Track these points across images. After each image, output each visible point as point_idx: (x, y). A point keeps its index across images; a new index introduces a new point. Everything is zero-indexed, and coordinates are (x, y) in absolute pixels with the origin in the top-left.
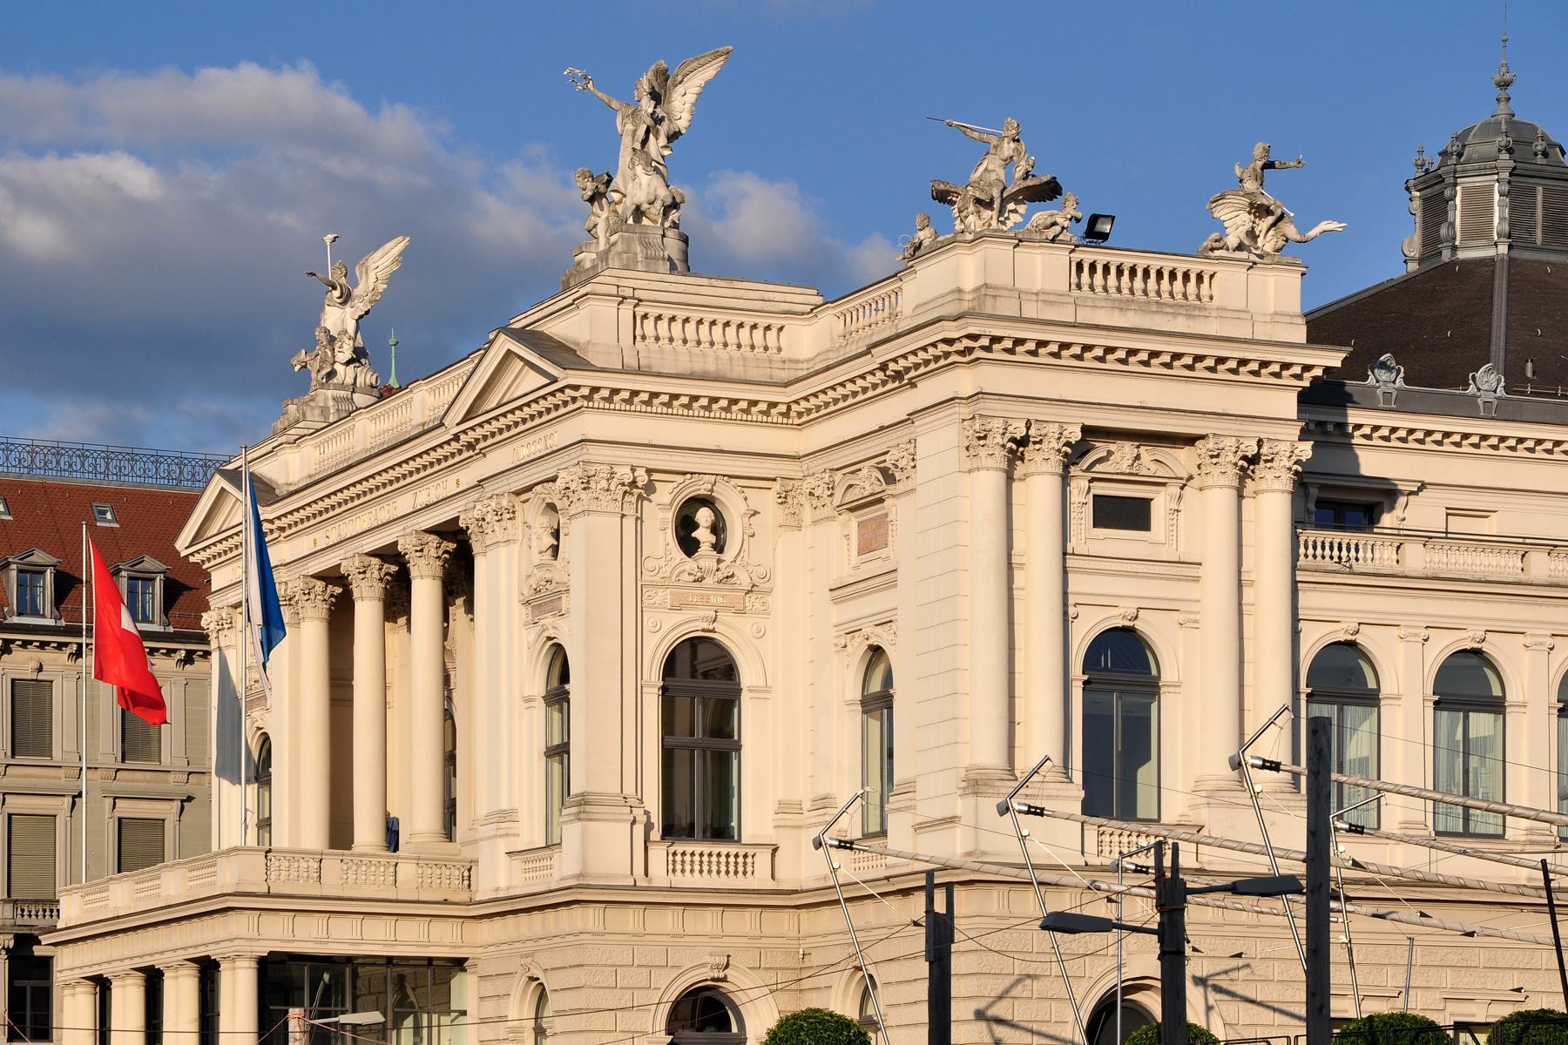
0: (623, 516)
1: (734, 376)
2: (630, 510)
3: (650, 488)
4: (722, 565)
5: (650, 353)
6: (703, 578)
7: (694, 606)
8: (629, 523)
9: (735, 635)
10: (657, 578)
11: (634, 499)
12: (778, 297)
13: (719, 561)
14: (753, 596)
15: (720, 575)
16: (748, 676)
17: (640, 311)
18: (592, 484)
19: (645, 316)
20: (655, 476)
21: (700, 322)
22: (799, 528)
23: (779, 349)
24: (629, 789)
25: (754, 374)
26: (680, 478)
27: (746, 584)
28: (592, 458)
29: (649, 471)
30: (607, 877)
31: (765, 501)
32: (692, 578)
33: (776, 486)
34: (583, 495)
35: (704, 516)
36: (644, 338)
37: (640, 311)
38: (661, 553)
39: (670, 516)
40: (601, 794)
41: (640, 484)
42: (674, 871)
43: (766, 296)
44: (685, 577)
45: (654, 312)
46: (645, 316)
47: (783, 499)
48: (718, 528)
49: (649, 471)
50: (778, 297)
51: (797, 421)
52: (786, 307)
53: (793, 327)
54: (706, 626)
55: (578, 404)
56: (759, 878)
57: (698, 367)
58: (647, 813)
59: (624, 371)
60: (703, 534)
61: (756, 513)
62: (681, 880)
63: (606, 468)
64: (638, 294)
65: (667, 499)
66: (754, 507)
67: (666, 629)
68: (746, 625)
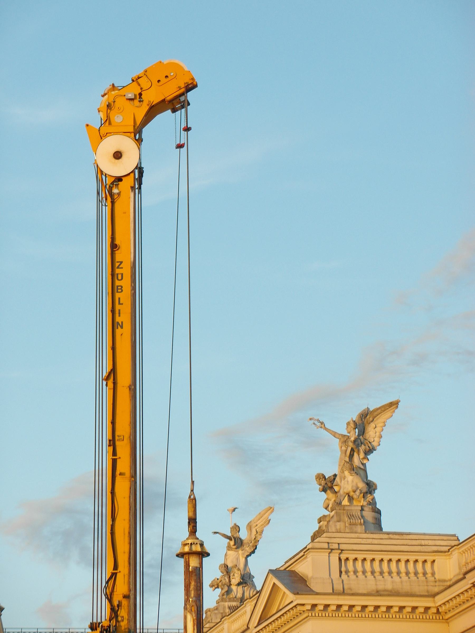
5: (351, 582)
12: (430, 543)
21: (382, 560)
23: (433, 574)
25: (417, 589)
36: (347, 572)
37: (343, 557)
43: (423, 542)
45: (352, 556)
46: (347, 559)
50: (430, 543)
51: (447, 617)
52: (435, 548)
53: (439, 559)
55: (306, 615)
57: (381, 587)
59: (334, 593)
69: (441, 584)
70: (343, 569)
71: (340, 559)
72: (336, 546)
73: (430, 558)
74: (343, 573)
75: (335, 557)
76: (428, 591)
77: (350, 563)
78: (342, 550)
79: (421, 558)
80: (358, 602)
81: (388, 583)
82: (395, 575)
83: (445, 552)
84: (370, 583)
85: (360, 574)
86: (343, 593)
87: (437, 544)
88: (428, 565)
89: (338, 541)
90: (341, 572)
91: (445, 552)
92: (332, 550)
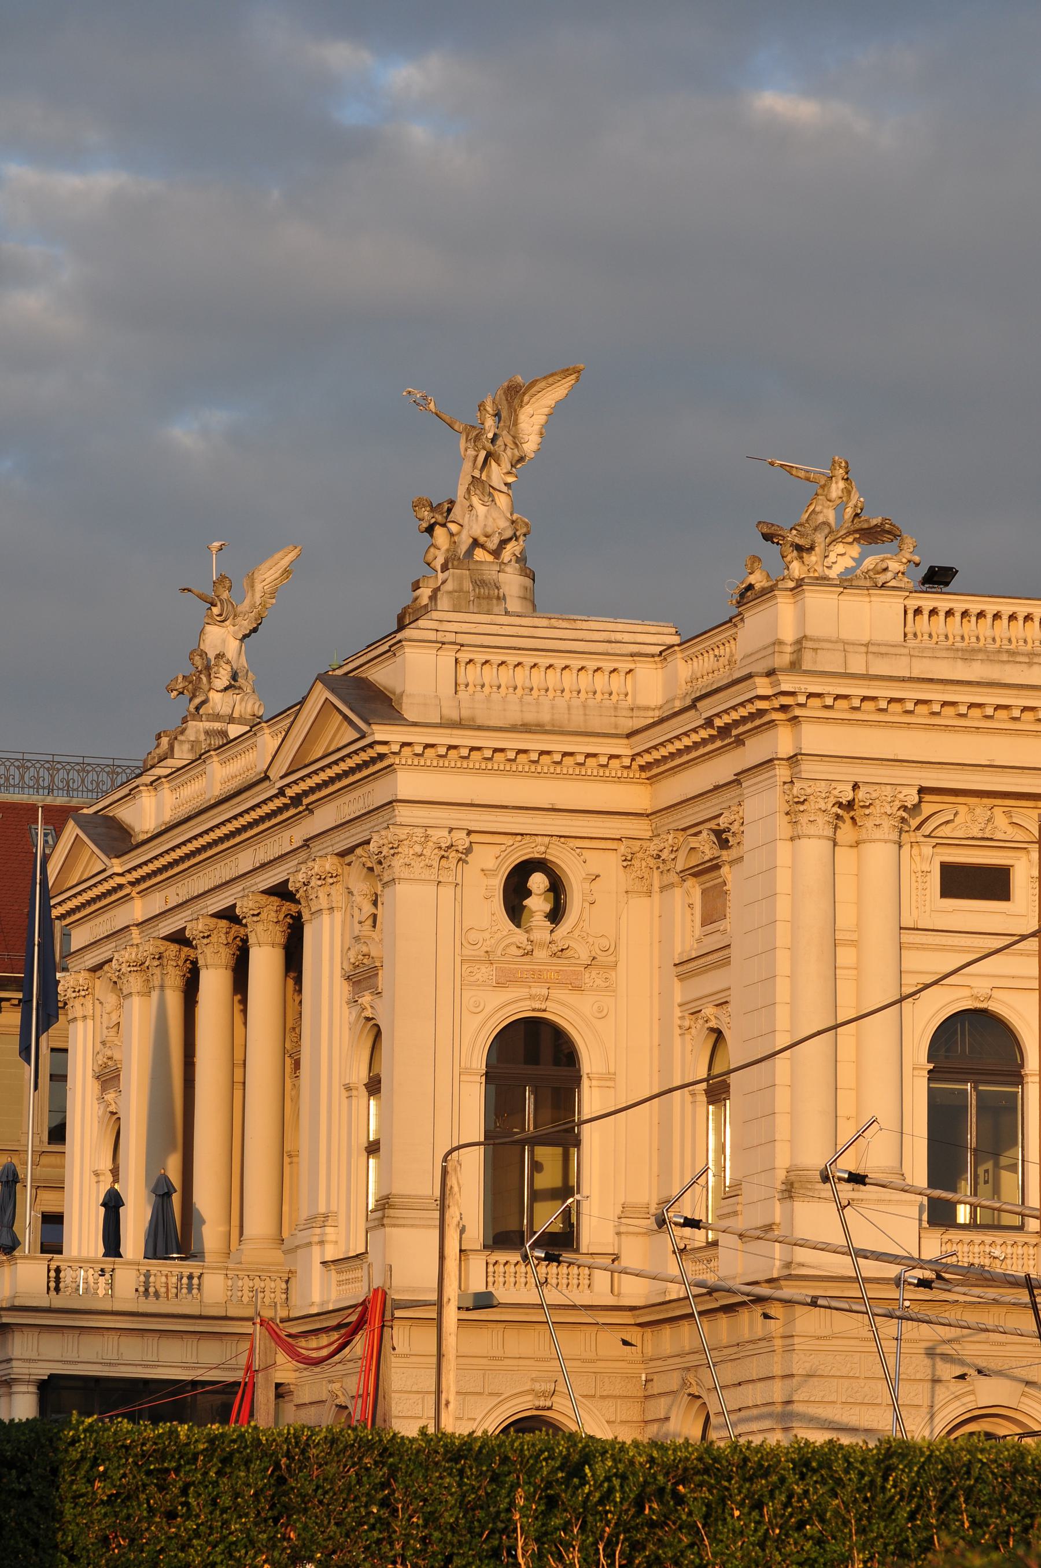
15: (554, 948)
20: (474, 838)
25: (596, 725)
33: (622, 848)
35: (538, 882)
43: (613, 637)
44: (514, 950)
50: (627, 637)
52: (635, 648)
54: (537, 1006)
60: (538, 904)
69: (642, 713)
76: (616, 727)
80: (488, 741)
83: (653, 656)
87: (639, 641)
91: (653, 656)
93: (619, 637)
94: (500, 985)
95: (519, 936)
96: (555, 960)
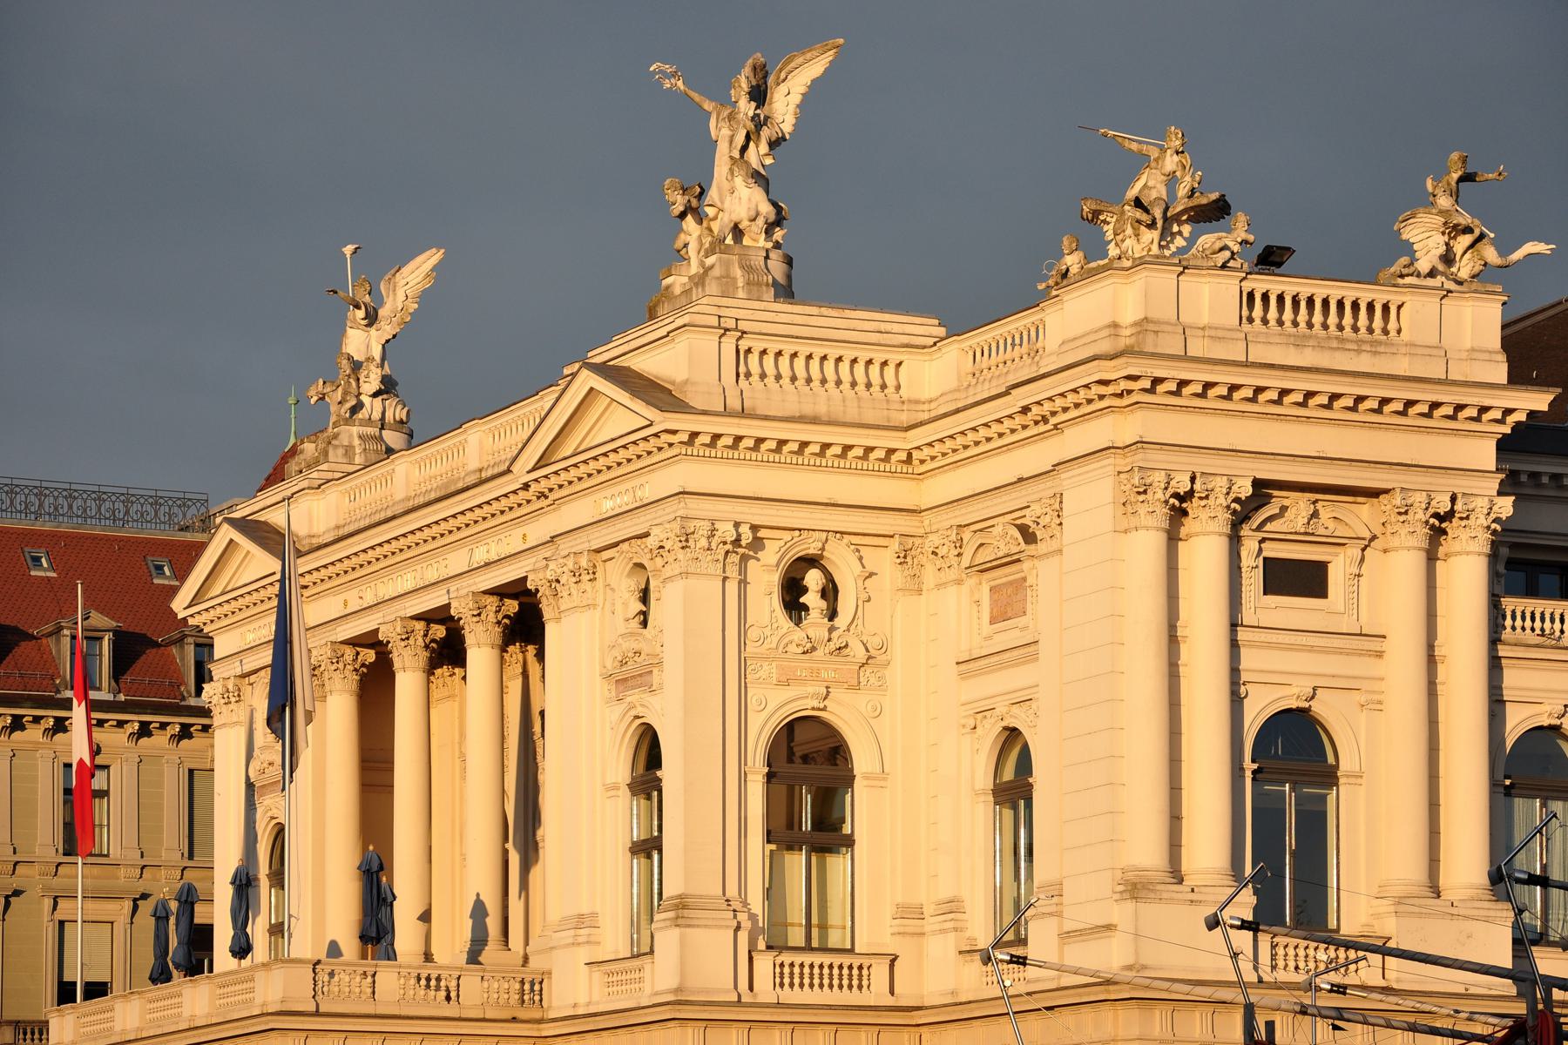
0: (725, 579)
1: (848, 419)
2: (733, 572)
3: (757, 544)
4: (835, 635)
5: (757, 394)
6: (814, 649)
7: (802, 681)
8: (732, 587)
9: (845, 716)
10: (763, 650)
11: (736, 558)
12: (896, 328)
13: (831, 630)
14: (868, 669)
15: (832, 646)
16: (862, 761)
17: (744, 345)
18: (691, 543)
19: (749, 351)
22: (920, 592)
23: (898, 387)
24: (732, 891)
26: (787, 536)
27: (861, 654)
28: (691, 513)
29: (755, 528)
30: (708, 991)
31: (883, 560)
32: (800, 650)
33: (895, 545)
34: (681, 554)
35: (813, 579)
36: (748, 375)
37: (744, 345)
38: (766, 621)
39: (775, 578)
40: (701, 897)
41: (743, 543)
42: (782, 985)
43: (883, 327)
44: (792, 648)
45: (758, 346)
46: (749, 351)
47: (904, 557)
48: (830, 592)
49: (755, 528)
50: (896, 328)
54: (815, 704)
56: (876, 992)
57: (808, 410)
58: (753, 917)
59: (726, 413)
60: (812, 599)
61: (871, 575)
62: (787, 996)
63: (707, 525)
64: (743, 325)
65: (773, 560)
66: (869, 568)
67: (770, 708)
68: (862, 701)
70: (742, 369)
71: (738, 351)
72: (731, 324)
73: (894, 358)
74: (742, 377)
75: (729, 344)
77: (754, 359)
78: (744, 333)
79: (879, 357)
81: (821, 401)
82: (831, 385)
84: (789, 399)
85: (770, 380)
86: (743, 413)
88: (890, 371)
89: (741, 314)
90: (738, 375)
92: (727, 330)
93: (888, 327)
94: (779, 683)
95: (798, 635)
96: (833, 658)
